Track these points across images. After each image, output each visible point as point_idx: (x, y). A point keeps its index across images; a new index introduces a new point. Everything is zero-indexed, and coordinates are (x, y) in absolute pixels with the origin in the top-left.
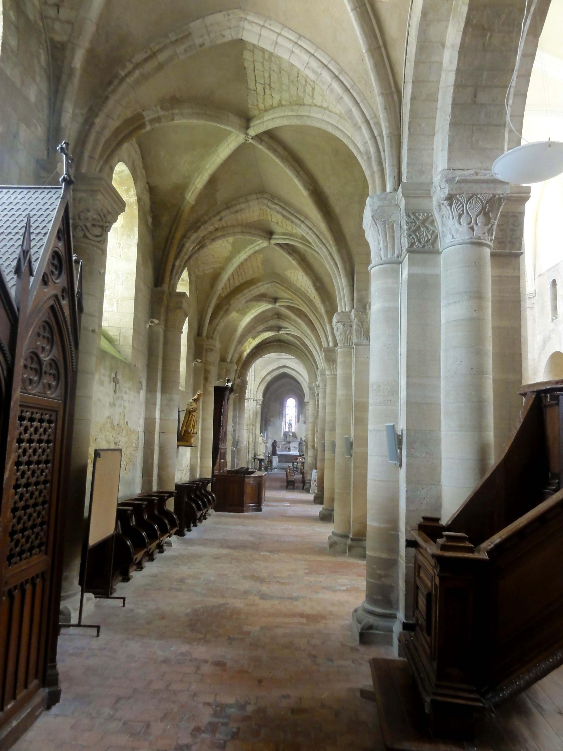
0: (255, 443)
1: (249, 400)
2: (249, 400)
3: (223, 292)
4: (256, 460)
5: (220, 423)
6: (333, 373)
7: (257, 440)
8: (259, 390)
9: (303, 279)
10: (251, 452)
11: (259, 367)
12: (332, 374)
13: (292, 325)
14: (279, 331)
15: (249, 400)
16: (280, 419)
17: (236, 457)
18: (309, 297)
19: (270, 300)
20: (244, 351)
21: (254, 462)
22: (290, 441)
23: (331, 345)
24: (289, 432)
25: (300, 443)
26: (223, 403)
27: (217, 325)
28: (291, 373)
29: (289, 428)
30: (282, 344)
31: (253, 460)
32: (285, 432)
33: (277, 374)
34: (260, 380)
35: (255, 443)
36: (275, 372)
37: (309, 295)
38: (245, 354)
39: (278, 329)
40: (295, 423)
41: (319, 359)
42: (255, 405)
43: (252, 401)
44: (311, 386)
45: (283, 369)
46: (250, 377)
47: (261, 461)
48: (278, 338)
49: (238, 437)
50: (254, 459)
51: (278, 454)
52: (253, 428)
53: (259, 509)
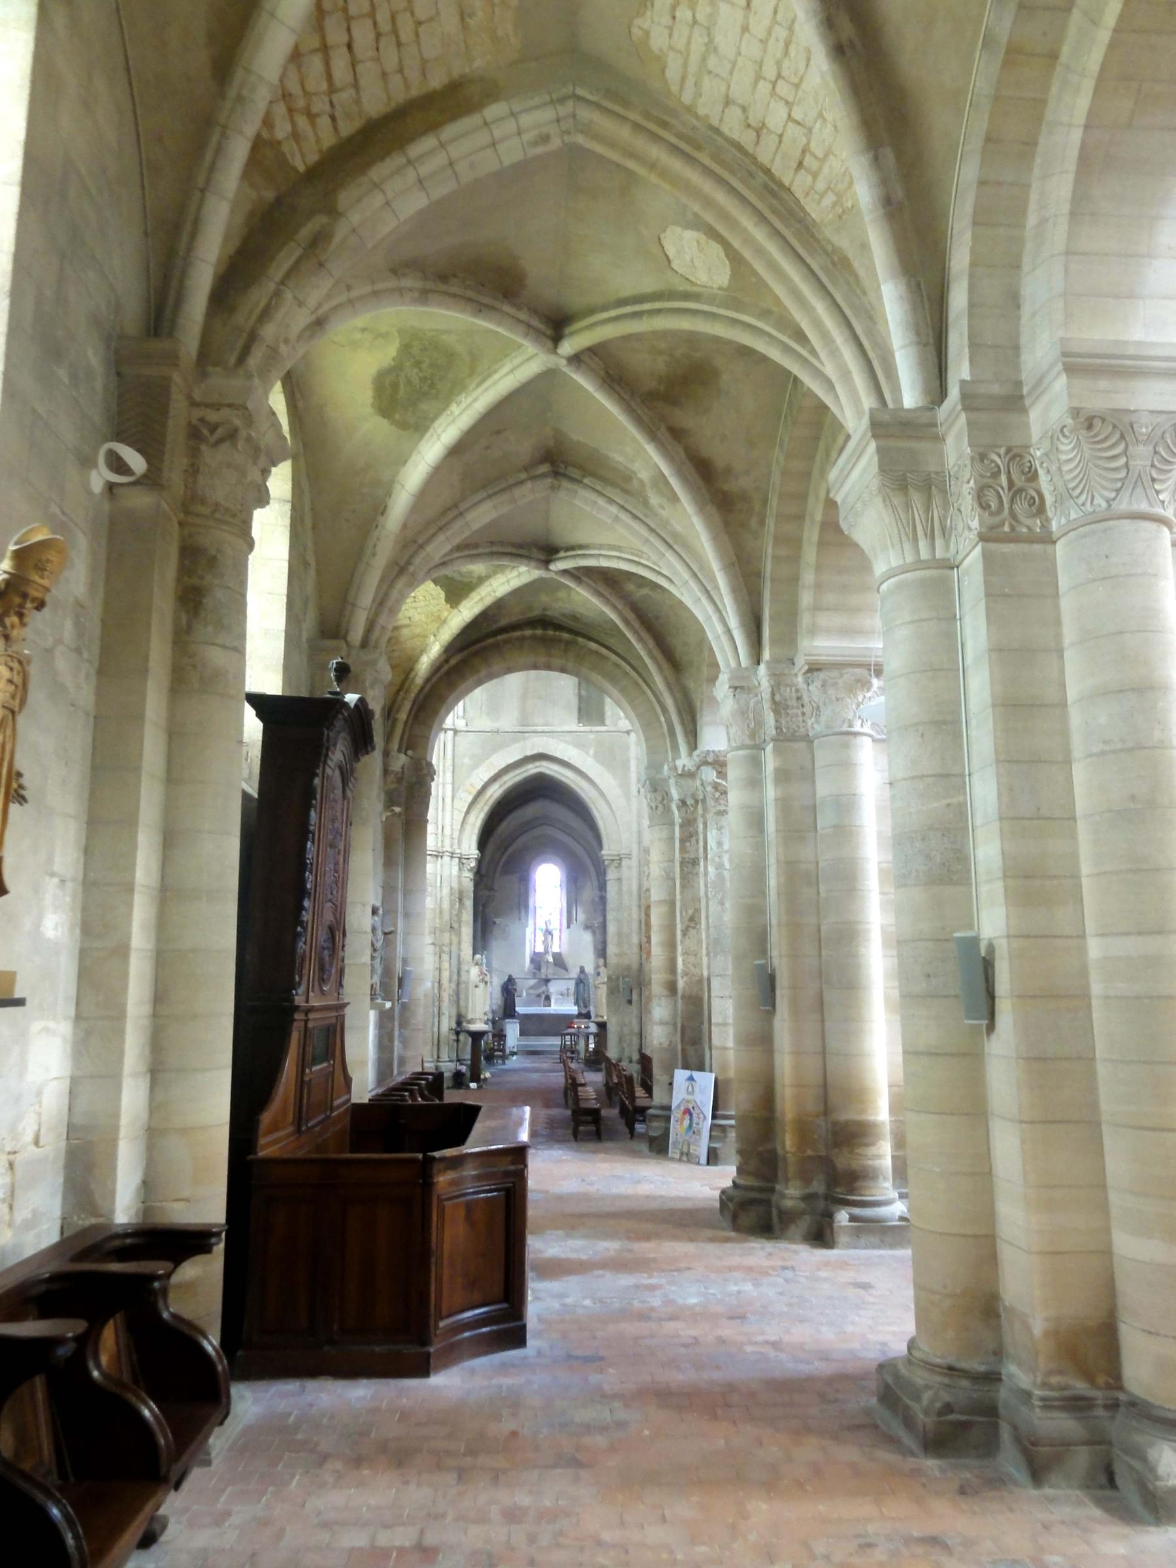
0: (458, 984)
1: (437, 856)
3: (295, 135)
4: (462, 1037)
5: (302, 881)
6: (925, 554)
7: (463, 974)
8: (468, 827)
9: (745, 29)
11: (466, 761)
12: (919, 564)
13: (611, 501)
14: (546, 563)
15: (438, 855)
16: (520, 919)
17: (396, 1033)
18: (768, 172)
19: (536, 323)
21: (458, 1041)
22: (550, 977)
23: (910, 397)
24: (546, 952)
25: (581, 982)
26: (317, 781)
27: (266, 314)
29: (543, 942)
30: (551, 632)
31: (454, 1037)
32: (535, 953)
34: (470, 798)
35: (458, 984)
36: (512, 774)
37: (764, 157)
38: (425, 664)
39: (543, 557)
40: (560, 930)
41: (720, 629)
43: (446, 859)
44: (658, 776)
45: (538, 764)
46: (441, 787)
47: (477, 1036)
48: (536, 613)
49: (405, 962)
50: (458, 1033)
51: (520, 1012)
53: (517, 1338)
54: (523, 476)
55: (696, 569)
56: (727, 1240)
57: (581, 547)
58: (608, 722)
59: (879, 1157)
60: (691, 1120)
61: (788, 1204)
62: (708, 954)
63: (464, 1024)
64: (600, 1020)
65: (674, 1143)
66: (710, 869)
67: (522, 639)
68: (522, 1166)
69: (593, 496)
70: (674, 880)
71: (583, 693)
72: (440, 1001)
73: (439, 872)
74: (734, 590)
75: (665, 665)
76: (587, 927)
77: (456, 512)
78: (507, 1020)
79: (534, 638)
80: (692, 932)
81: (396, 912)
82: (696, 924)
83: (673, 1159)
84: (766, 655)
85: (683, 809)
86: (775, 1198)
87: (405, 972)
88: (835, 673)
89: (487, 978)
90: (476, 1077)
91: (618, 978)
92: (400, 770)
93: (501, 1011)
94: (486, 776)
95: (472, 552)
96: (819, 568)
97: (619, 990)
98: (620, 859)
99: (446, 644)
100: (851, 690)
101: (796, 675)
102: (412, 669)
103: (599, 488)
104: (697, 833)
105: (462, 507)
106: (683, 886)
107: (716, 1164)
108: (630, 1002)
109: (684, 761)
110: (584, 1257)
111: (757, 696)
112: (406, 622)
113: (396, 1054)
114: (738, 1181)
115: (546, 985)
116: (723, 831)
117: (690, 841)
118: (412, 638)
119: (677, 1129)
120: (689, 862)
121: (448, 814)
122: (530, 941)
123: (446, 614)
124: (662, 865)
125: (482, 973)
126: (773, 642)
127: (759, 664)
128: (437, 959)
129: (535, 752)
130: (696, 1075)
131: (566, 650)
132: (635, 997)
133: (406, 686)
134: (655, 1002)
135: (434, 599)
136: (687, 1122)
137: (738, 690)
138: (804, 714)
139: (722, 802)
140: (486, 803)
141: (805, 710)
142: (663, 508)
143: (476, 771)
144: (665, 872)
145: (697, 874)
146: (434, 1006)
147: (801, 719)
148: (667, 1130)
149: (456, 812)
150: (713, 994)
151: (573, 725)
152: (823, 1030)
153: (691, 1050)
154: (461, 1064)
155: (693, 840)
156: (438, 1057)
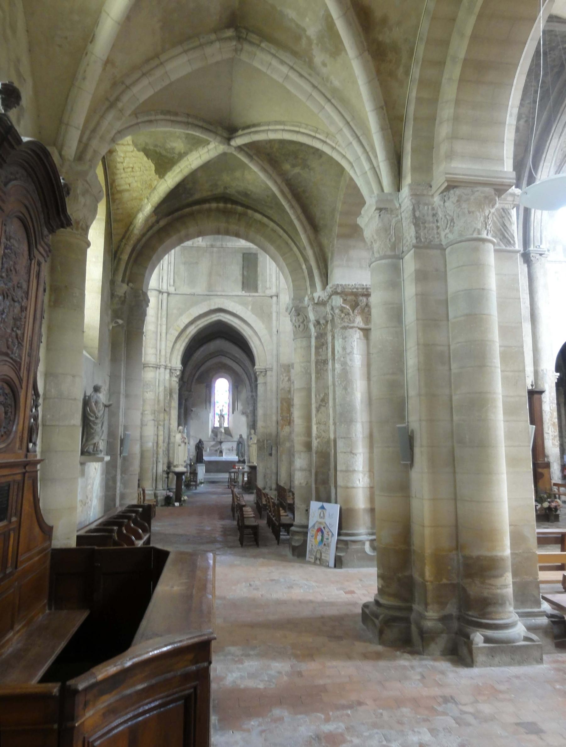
0: (169, 444)
1: (156, 368)
2: (156, 368)
4: (171, 475)
8: (175, 352)
11: (175, 311)
13: (282, 62)
15: (157, 367)
17: (119, 477)
20: (138, 212)
21: (168, 478)
22: (222, 440)
24: (221, 426)
25: (240, 443)
28: (232, 321)
30: (229, 206)
31: (165, 475)
32: (214, 428)
33: (206, 323)
34: (177, 334)
35: (169, 444)
36: (203, 320)
38: (140, 219)
39: (225, 135)
40: (228, 415)
42: (167, 376)
43: (162, 370)
44: (301, 305)
45: (218, 314)
47: (179, 475)
48: (220, 190)
49: (126, 428)
50: (168, 473)
52: (164, 418)
54: (213, 37)
55: (349, 119)
56: (378, 656)
57: (254, 126)
58: (259, 291)
59: (506, 586)
60: (322, 536)
61: (429, 624)
62: (335, 424)
63: (172, 468)
64: (251, 464)
65: (310, 551)
66: (337, 366)
67: (210, 210)
68: (206, 664)
69: (268, 58)
70: (310, 374)
71: (245, 273)
72: (157, 454)
74: (383, 129)
75: (308, 227)
76: (243, 413)
77: (156, 62)
78: (198, 464)
79: (218, 210)
80: (323, 409)
81: (119, 393)
82: (326, 404)
83: (309, 562)
84: (407, 180)
85: (318, 326)
86: (413, 616)
87: (125, 434)
88: (468, 191)
89: (186, 441)
90: (178, 499)
91: (263, 441)
92: (123, 295)
93: (194, 460)
94: (187, 321)
95: (172, 118)
96: (458, 102)
97: (264, 448)
98: (266, 371)
99: (156, 205)
100: (480, 205)
101: (432, 195)
102: (131, 223)
103: (273, 51)
104: (327, 343)
105: (163, 58)
106: (317, 378)
107: (341, 567)
108: (271, 455)
109: (319, 293)
110: (261, 686)
111: (397, 216)
112: (127, 187)
113: (118, 492)
114: (382, 601)
115: (221, 445)
116: (347, 339)
117: (322, 348)
118: (132, 200)
119: (312, 542)
120: (321, 362)
121: (163, 343)
122: (212, 421)
123: (155, 182)
124: (303, 365)
125: (183, 437)
126: (414, 169)
127: (399, 191)
129: (216, 307)
130: (326, 505)
131: (239, 220)
132: (274, 452)
133: (127, 236)
134: (297, 456)
135: (146, 170)
136: (319, 537)
137: (383, 211)
138: (438, 227)
139: (346, 320)
140: (186, 337)
141: (439, 224)
142: (324, 65)
144: (305, 368)
145: (327, 370)
146: (153, 457)
147: (435, 231)
148: (305, 542)
149: (168, 342)
150: (339, 450)
151: (239, 292)
152: (455, 481)
153: (322, 489)
154: (170, 491)
155: (324, 348)
156: (156, 487)
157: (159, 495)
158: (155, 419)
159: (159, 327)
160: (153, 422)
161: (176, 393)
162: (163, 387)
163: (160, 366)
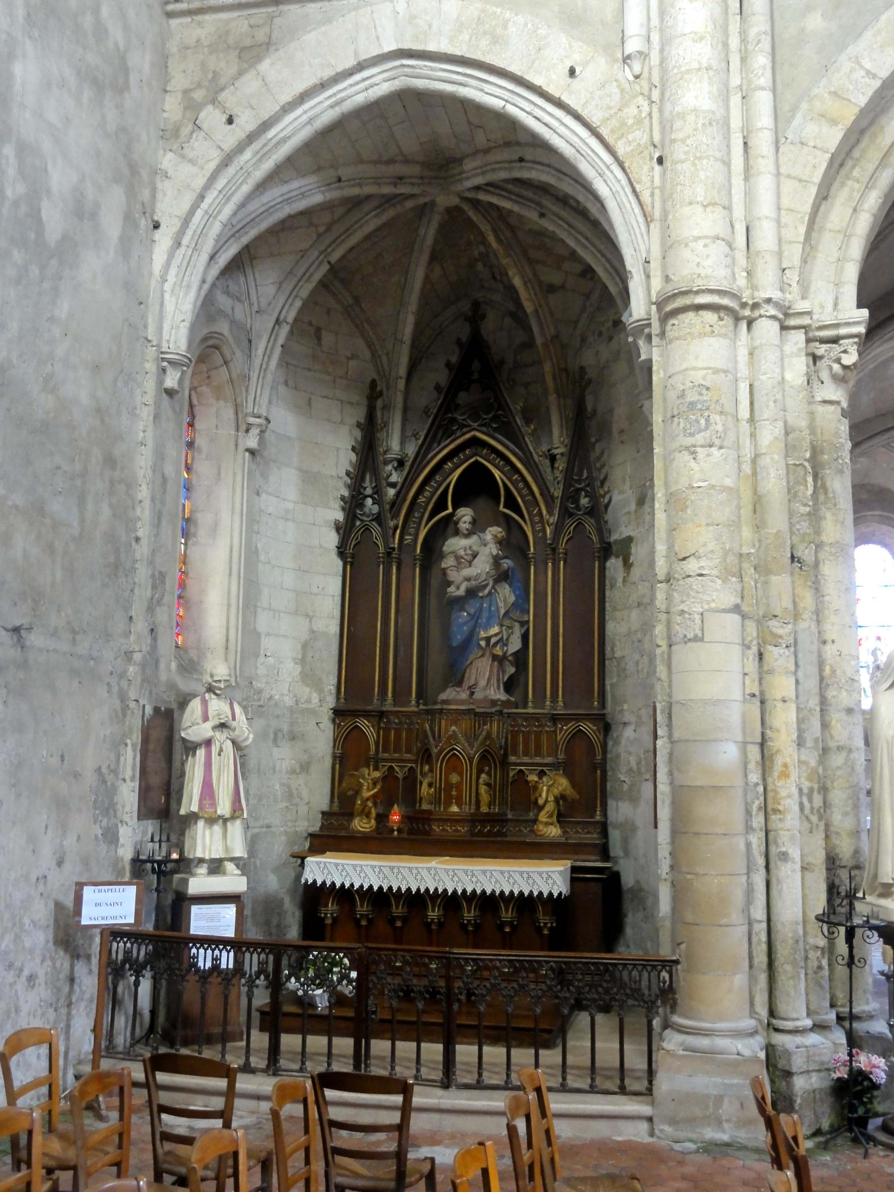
1: (737, 319)
10: (795, 853)
11: (815, 22)
34: (833, 137)
42: (798, 367)
43: (767, 329)
73: (743, 369)
121: (765, 184)
128: (752, 665)
143: (851, 50)
146: (749, 829)
149: (788, 186)
156: (772, 1013)
157: (798, 1063)
158: (745, 608)
159: (735, 100)
160: (737, 618)
161: (841, 472)
162: (780, 424)
163: (755, 306)
